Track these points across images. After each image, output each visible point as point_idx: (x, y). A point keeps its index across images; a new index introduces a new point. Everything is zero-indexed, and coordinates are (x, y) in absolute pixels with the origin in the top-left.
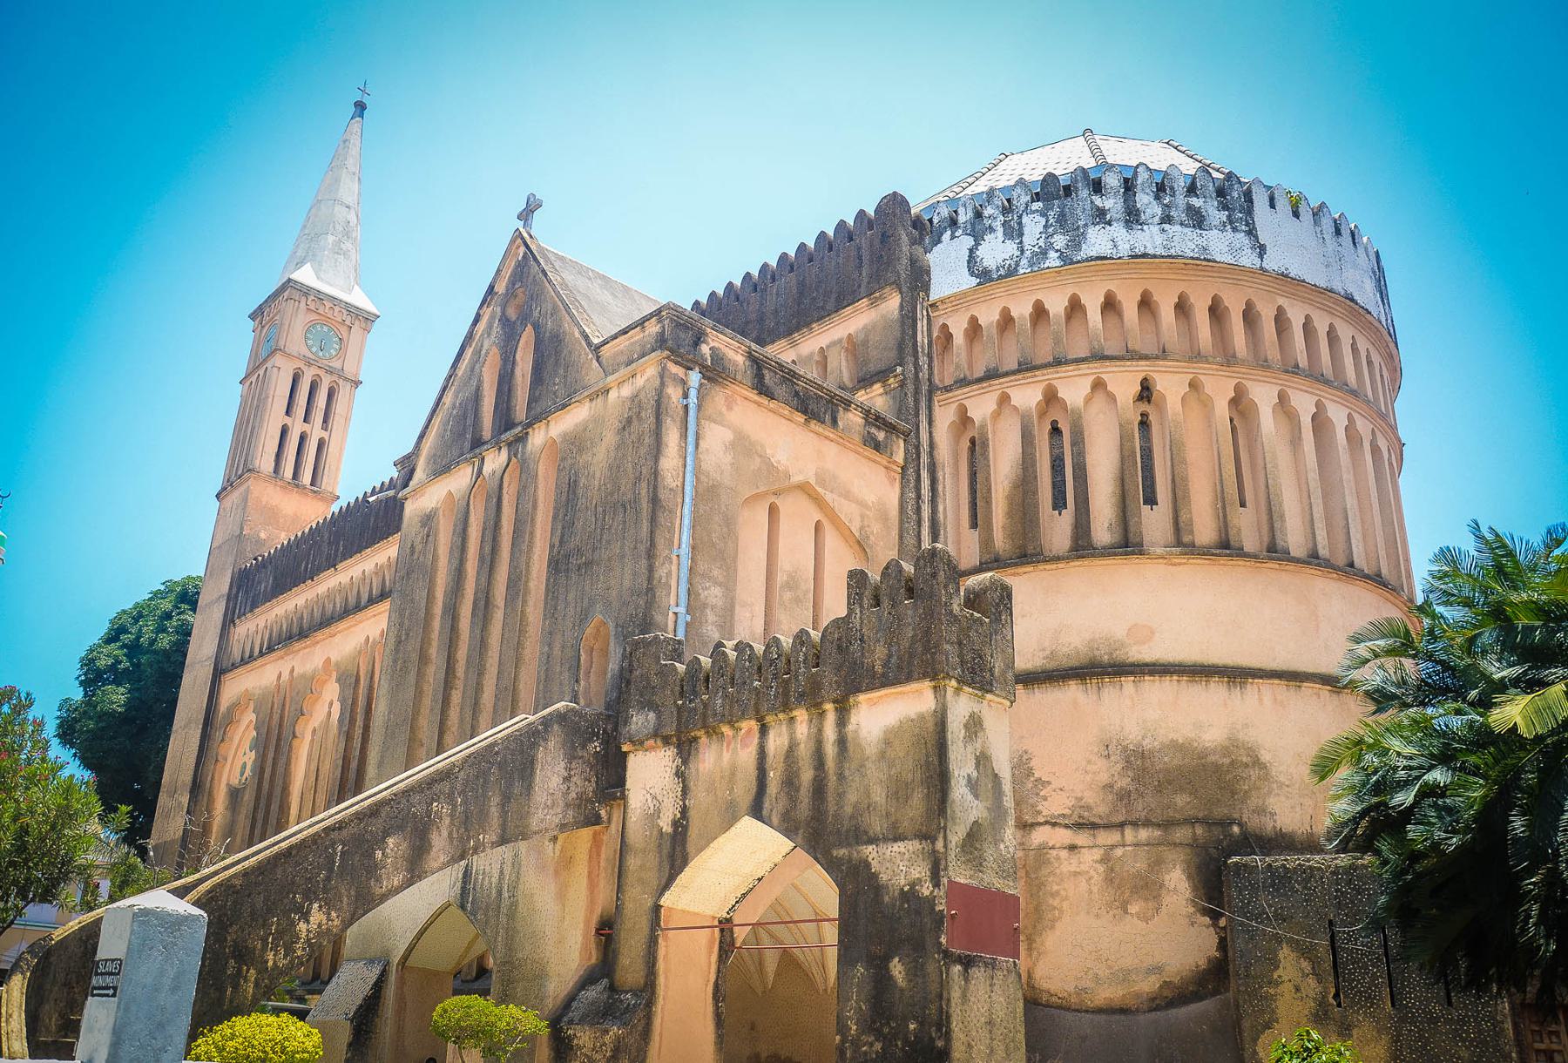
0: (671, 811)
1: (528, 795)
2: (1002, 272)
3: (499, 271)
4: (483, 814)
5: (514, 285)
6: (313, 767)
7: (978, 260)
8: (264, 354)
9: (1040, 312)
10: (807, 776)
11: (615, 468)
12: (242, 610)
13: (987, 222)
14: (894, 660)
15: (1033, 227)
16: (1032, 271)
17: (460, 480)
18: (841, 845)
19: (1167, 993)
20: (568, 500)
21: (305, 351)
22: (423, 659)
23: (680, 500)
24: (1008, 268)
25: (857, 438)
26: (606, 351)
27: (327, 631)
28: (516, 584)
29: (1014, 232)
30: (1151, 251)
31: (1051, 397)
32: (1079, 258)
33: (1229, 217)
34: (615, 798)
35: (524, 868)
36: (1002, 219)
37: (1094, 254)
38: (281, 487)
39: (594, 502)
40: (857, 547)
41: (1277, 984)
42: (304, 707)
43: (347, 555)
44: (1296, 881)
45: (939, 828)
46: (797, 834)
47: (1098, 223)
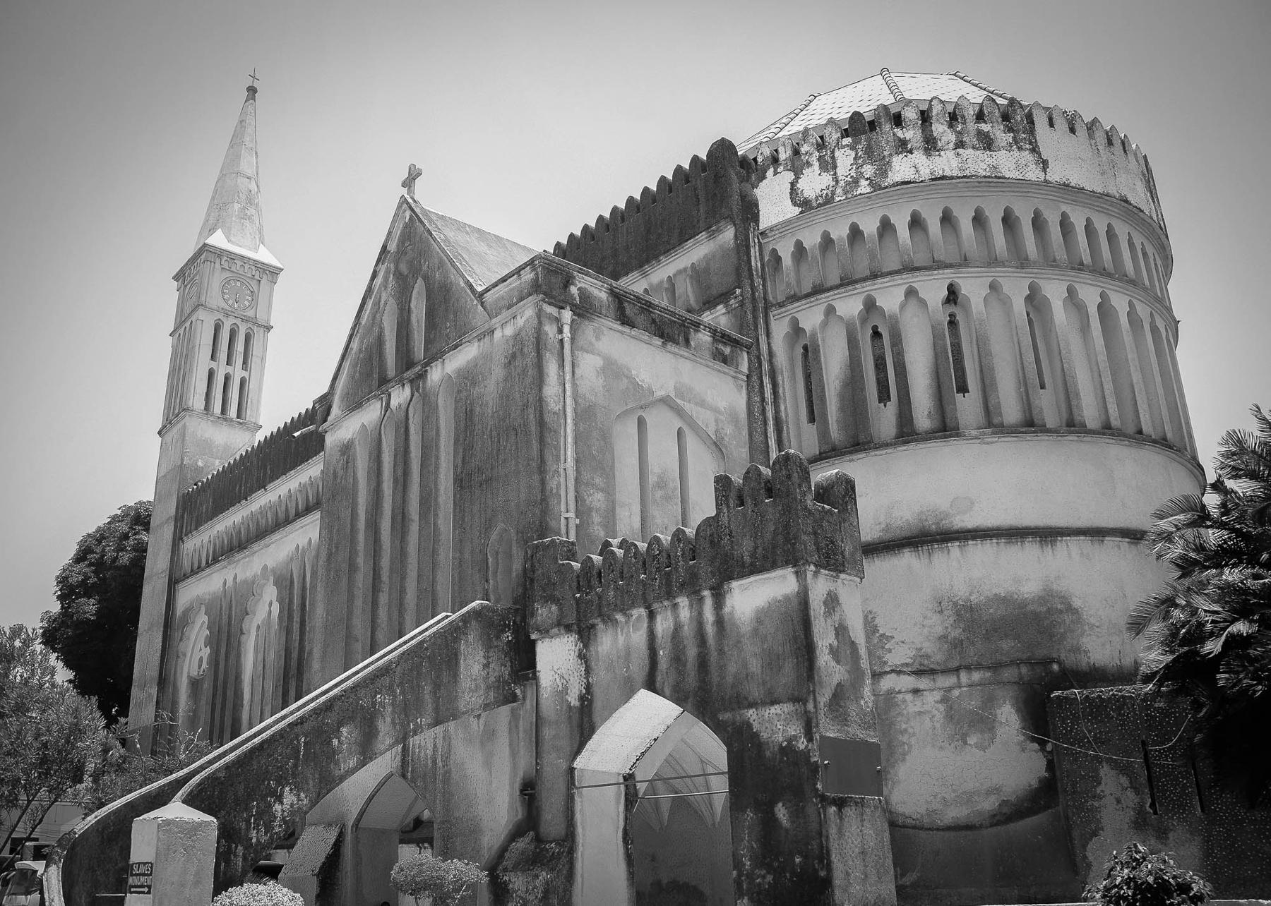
0: (577, 688)
1: (455, 682)
2: (821, 201)
3: (390, 233)
4: (419, 700)
5: (403, 244)
6: (260, 657)
7: (799, 191)
8: (188, 310)
9: (855, 233)
10: (692, 652)
11: (505, 397)
12: (189, 528)
13: (804, 158)
14: (760, 551)
15: (845, 159)
16: (847, 198)
17: (371, 414)
18: (726, 710)
20: (466, 427)
22: (353, 567)
23: (562, 421)
24: (826, 197)
25: (707, 355)
26: (489, 297)
27: (262, 543)
28: (428, 501)
29: (828, 165)
30: (948, 173)
31: (870, 305)
32: (886, 184)
33: (1014, 138)
34: (528, 679)
35: (454, 742)
36: (817, 154)
37: (899, 179)
38: (212, 421)
39: (489, 430)
40: (714, 447)
41: (1100, 798)
42: (248, 606)
43: (274, 477)
44: (1112, 710)
45: (809, 692)
46: (687, 703)
47: (901, 153)
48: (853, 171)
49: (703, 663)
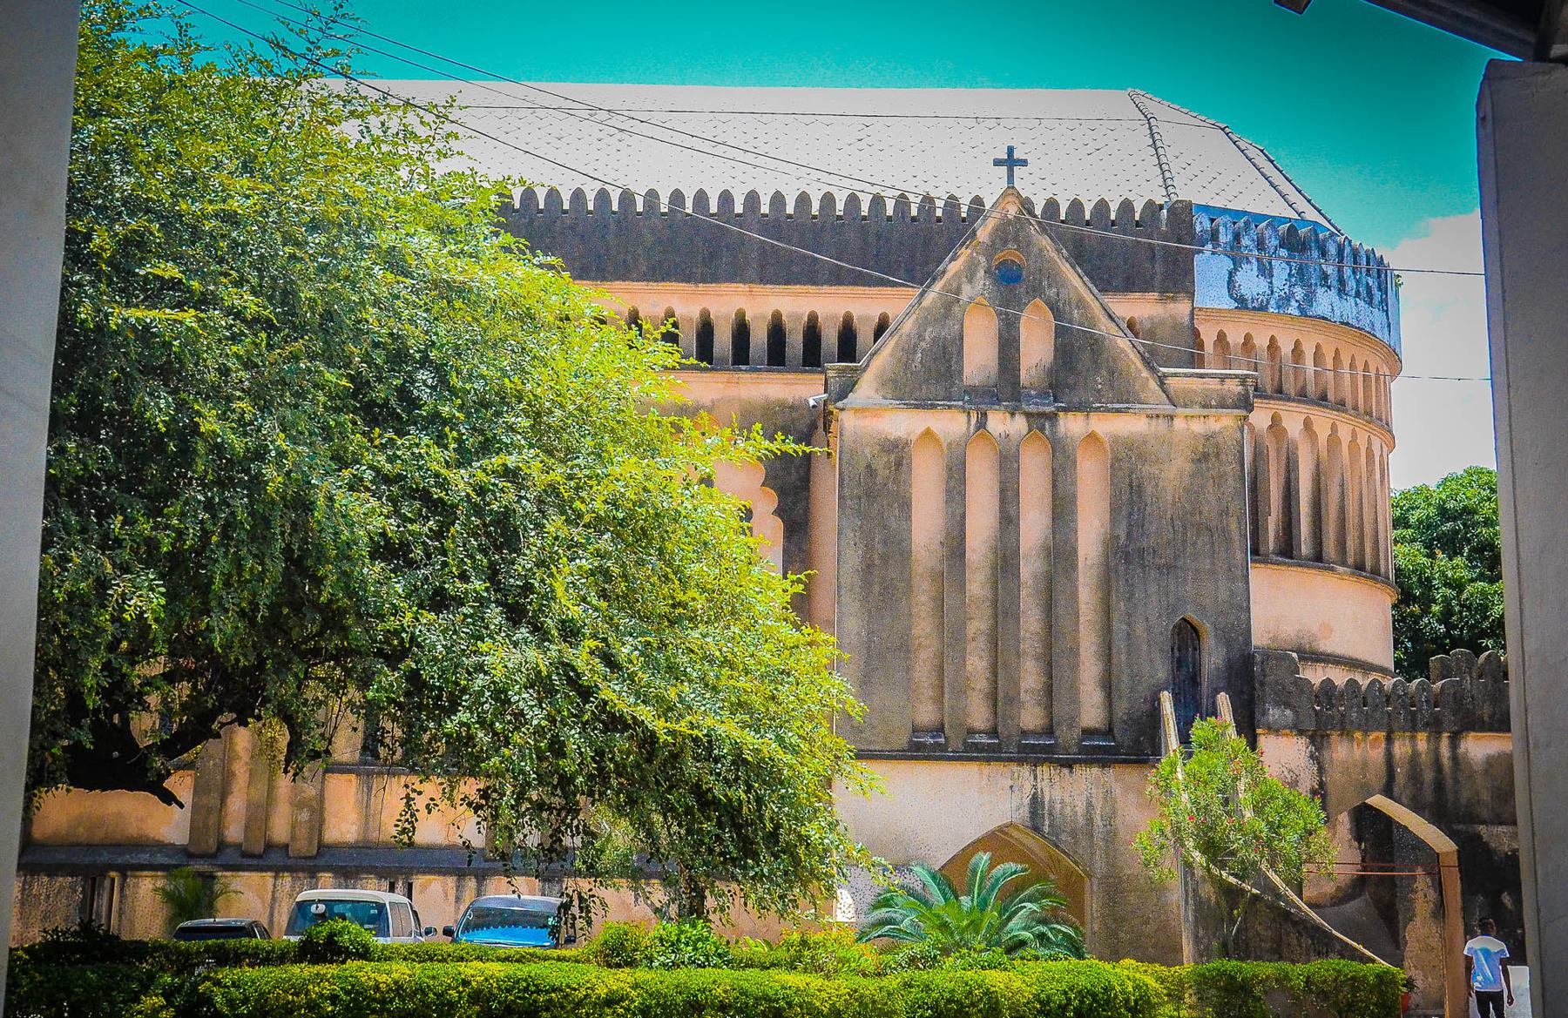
2: (1256, 304)
7: (1237, 285)
10: (1428, 776)
15: (1281, 272)
18: (1459, 823)
19: (1340, 895)
20: (1131, 503)
31: (1276, 421)
48: (1286, 287)
49: (1439, 785)
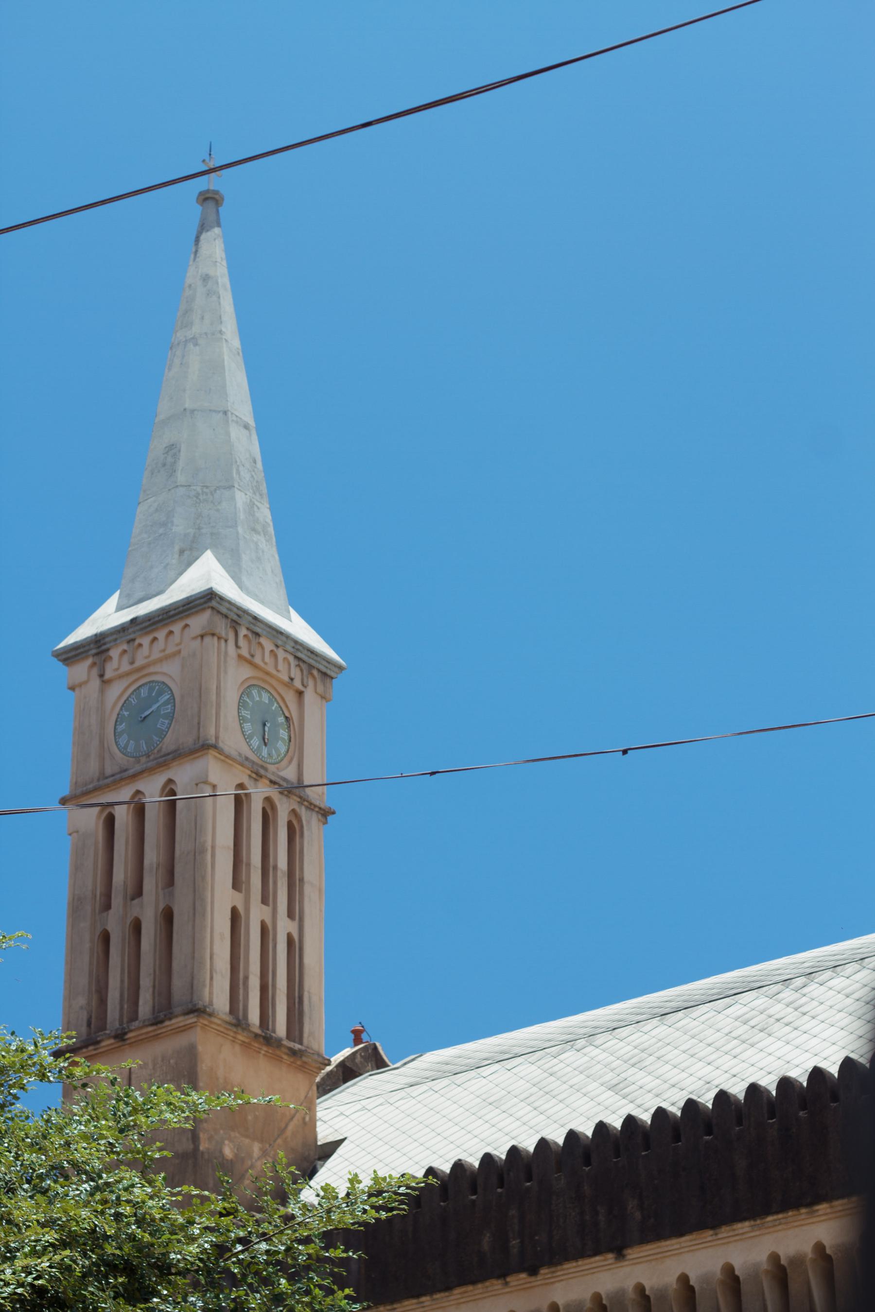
21: (246, 751)
38: (243, 1044)
